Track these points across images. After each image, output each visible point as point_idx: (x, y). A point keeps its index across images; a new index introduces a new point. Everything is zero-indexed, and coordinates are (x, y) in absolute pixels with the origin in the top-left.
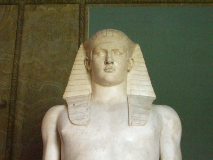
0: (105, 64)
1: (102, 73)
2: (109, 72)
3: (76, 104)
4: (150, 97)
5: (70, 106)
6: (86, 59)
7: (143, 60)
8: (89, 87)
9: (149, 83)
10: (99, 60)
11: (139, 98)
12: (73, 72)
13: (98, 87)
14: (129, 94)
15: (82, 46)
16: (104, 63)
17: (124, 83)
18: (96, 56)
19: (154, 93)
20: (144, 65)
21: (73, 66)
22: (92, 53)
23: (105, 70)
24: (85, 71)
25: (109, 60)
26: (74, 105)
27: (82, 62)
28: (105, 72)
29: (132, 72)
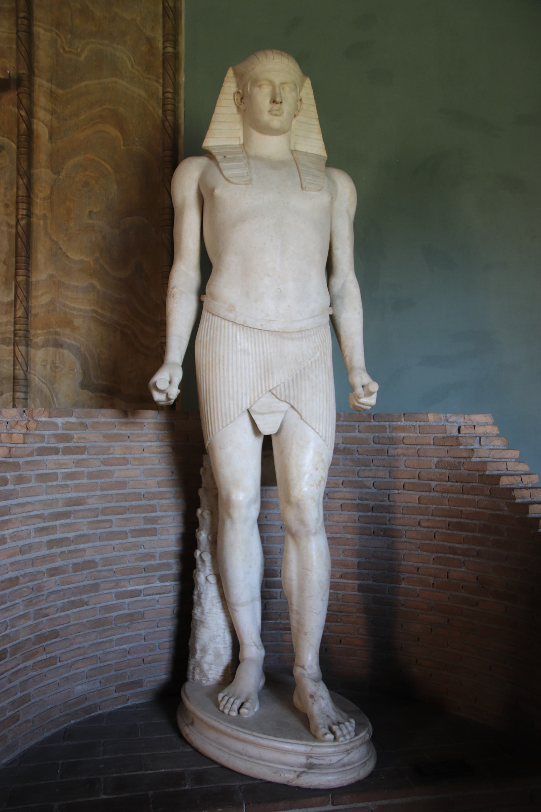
0: (270, 102)
1: (266, 117)
2: (276, 115)
3: (227, 157)
4: (320, 156)
5: (219, 158)
6: (238, 92)
7: (313, 102)
8: (241, 134)
9: (320, 137)
10: (262, 97)
11: (306, 154)
12: (218, 110)
13: (256, 135)
14: (293, 149)
15: (230, 72)
16: (269, 101)
17: (287, 134)
18: (256, 90)
19: (325, 151)
20: (314, 109)
21: (218, 101)
22: (251, 85)
23: (270, 111)
24: (234, 110)
25: (278, 100)
26: (225, 157)
27: (232, 97)
28: (272, 114)
29: (298, 118)
